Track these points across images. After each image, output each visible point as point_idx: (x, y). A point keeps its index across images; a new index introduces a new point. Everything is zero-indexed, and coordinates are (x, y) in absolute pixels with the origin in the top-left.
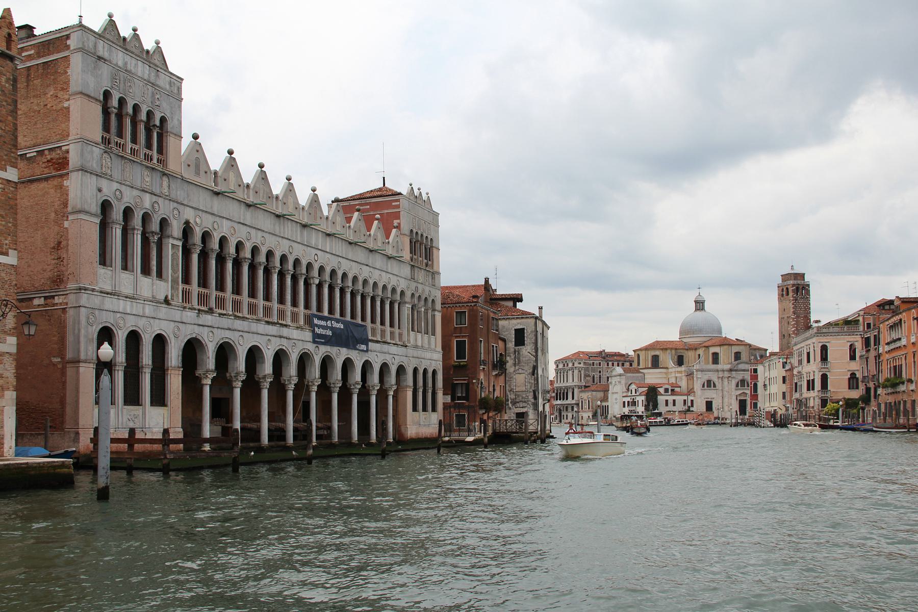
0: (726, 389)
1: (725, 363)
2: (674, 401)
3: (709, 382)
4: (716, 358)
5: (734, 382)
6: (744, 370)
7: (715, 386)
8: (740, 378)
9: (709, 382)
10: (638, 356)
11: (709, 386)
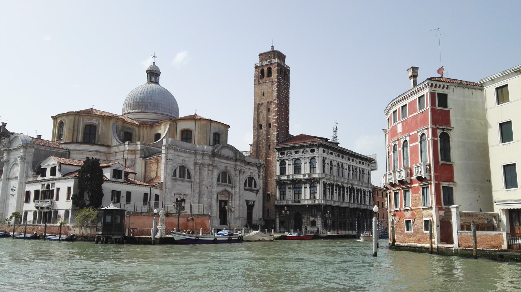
0: (206, 182)
1: (201, 144)
2: (129, 194)
3: (183, 168)
4: (187, 135)
5: (216, 173)
6: (228, 158)
7: (189, 177)
8: (222, 168)
9: (183, 168)
10: (61, 124)
11: (182, 176)
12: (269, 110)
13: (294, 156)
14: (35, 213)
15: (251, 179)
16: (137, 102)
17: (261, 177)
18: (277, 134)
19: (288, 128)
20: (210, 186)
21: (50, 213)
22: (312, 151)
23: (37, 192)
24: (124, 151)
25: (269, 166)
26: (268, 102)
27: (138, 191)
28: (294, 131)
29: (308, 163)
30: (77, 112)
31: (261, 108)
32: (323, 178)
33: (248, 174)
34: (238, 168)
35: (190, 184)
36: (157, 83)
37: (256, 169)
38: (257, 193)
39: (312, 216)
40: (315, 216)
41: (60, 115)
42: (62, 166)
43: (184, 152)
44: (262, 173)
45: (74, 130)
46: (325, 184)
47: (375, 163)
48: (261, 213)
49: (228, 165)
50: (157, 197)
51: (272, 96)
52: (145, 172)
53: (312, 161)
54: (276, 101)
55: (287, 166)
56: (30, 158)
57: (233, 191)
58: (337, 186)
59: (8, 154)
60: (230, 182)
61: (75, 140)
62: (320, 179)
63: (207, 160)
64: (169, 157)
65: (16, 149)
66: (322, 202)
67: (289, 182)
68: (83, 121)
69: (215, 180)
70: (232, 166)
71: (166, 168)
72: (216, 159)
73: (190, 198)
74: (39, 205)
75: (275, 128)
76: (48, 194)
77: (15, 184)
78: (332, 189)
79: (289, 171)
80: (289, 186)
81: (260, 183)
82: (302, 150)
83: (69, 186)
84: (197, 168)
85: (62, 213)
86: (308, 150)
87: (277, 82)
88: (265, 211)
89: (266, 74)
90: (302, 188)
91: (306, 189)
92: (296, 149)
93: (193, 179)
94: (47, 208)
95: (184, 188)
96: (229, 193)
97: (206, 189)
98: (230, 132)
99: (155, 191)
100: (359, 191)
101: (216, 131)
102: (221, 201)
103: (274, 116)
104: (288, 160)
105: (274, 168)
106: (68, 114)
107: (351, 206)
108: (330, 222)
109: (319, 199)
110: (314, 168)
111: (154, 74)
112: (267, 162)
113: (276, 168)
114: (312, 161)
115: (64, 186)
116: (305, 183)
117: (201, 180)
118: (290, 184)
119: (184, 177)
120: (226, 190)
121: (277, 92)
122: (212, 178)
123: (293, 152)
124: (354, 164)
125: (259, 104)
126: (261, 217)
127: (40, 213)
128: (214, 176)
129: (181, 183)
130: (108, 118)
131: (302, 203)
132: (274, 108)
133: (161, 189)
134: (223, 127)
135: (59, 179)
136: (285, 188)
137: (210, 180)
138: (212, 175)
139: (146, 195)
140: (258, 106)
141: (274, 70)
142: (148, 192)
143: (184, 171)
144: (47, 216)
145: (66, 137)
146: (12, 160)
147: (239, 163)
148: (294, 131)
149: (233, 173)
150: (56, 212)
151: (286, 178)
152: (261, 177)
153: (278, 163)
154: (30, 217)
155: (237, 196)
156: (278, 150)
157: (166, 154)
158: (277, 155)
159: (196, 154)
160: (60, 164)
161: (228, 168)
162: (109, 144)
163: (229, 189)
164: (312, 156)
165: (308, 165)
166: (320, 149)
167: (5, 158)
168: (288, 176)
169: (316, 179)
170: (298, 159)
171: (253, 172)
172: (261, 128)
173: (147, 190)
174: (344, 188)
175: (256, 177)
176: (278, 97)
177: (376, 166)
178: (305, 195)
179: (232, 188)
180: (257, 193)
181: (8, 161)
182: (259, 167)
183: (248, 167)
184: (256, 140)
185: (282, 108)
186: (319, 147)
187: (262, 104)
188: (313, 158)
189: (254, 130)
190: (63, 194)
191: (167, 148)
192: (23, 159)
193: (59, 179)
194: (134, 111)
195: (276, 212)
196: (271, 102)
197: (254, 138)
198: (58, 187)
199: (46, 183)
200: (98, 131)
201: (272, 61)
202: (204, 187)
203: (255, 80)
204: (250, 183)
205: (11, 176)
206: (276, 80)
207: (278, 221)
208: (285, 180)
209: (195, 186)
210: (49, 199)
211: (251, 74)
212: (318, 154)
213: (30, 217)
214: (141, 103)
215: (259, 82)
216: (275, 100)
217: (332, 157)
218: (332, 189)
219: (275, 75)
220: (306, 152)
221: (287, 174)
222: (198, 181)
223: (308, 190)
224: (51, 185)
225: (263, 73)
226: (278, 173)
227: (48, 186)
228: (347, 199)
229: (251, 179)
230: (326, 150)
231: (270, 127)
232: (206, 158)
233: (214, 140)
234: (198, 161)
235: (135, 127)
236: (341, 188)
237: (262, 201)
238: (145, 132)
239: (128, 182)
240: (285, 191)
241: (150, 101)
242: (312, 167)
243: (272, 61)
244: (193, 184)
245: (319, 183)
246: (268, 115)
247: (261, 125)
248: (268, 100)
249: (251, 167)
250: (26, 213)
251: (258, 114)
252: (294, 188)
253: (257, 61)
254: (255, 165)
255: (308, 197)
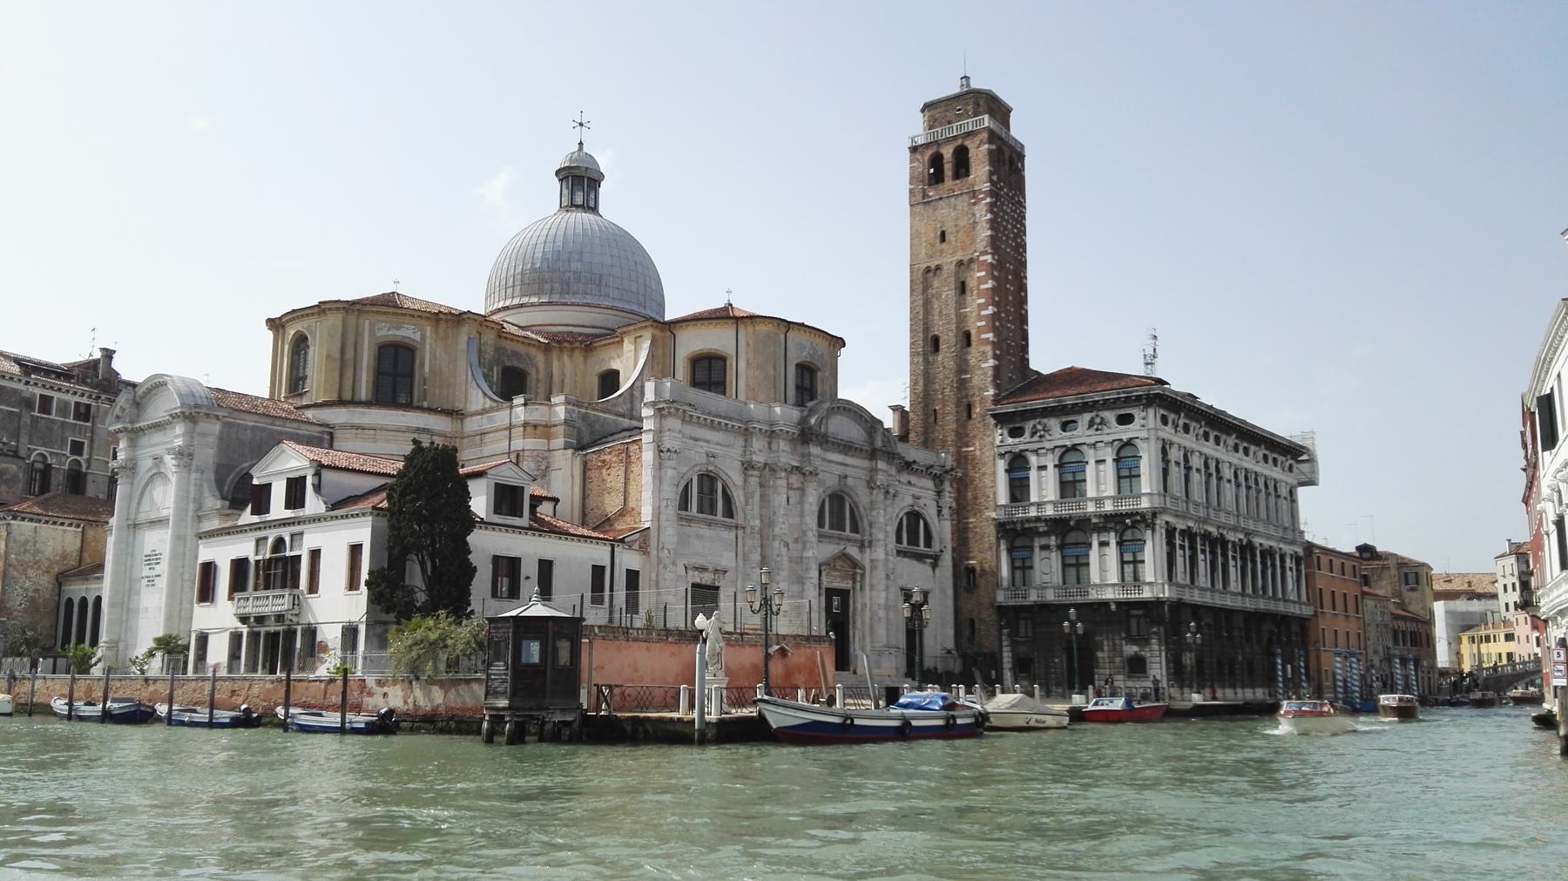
0: (781, 528)
2: (546, 567)
3: (708, 480)
6: (846, 447)
7: (729, 512)
8: (832, 482)
9: (708, 480)
10: (301, 342)
11: (707, 506)
12: (962, 288)
13: (1058, 436)
14: (236, 638)
15: (914, 516)
16: (533, 270)
17: (946, 512)
18: (996, 368)
19: (1025, 348)
20: (796, 540)
21: (290, 634)
22: (1125, 420)
23: (239, 566)
24: (510, 427)
25: (971, 473)
26: (960, 263)
27: (575, 558)
28: (1044, 358)
29: (1109, 461)
30: (354, 303)
31: (936, 283)
32: (1164, 510)
33: (905, 502)
34: (881, 479)
35: (733, 534)
36: (594, 209)
37: (929, 483)
38: (934, 566)
39: (1132, 640)
40: (1143, 641)
41: (296, 315)
42: (326, 474)
43: (713, 426)
44: (948, 499)
45: (344, 362)
46: (1170, 532)
47: (1312, 460)
48: (951, 632)
49: (849, 471)
50: (633, 577)
51: (973, 241)
52: (584, 497)
53: (1125, 456)
54: (989, 258)
55: (1033, 474)
56: (207, 454)
57: (865, 558)
58: (1206, 536)
59: (133, 445)
60: (855, 529)
61: (347, 396)
62: (1154, 515)
63: (785, 454)
64: (668, 443)
65: (158, 426)
66: (1166, 593)
67: (1042, 527)
68: (372, 332)
69: (812, 520)
70: (861, 473)
71: (658, 479)
72: (815, 450)
73: (734, 583)
74: (251, 608)
75: (989, 348)
76: (280, 571)
77: (158, 541)
78: (1193, 548)
79: (1040, 488)
80: (1044, 541)
81: (943, 530)
82: (1087, 417)
83: (355, 541)
84: (754, 481)
85: (331, 635)
86: (1110, 416)
87: (992, 193)
88: (965, 626)
89: (948, 168)
90: (1090, 545)
91: (1107, 550)
92: (1066, 414)
93: (739, 518)
94: (280, 618)
95: (713, 546)
96: (854, 564)
97: (784, 551)
98: (845, 359)
99: (629, 559)
100: (1268, 553)
101: (804, 356)
102: (830, 593)
103: (982, 307)
104: (1036, 451)
105: (987, 481)
106: (323, 308)
107: (1249, 604)
108: (1188, 659)
109: (1153, 582)
110: (1131, 476)
111: (580, 181)
112: (962, 459)
113: (994, 481)
114: (1125, 456)
115: (338, 543)
116: (1100, 529)
117: (768, 523)
118: (1046, 534)
119: (713, 512)
120: (844, 556)
121: (992, 228)
122: (802, 515)
123: (1054, 424)
124: (1248, 463)
125: (928, 270)
126: (951, 644)
127: (254, 636)
128: (807, 506)
129: (705, 531)
130: (449, 320)
131: (1094, 596)
132: (981, 281)
133: (644, 549)
134: (822, 346)
135: (316, 519)
136: (1031, 548)
137: (797, 520)
138: (801, 503)
139: (598, 571)
140: (925, 279)
141: (979, 154)
142: (607, 562)
143: (713, 491)
144: (279, 645)
145: (318, 383)
146: (146, 464)
147: (881, 465)
148: (1044, 358)
149: (863, 496)
150: (311, 632)
151: (1033, 513)
152: (946, 512)
153: (1001, 465)
154: (218, 652)
155: (880, 573)
156: (1001, 419)
157: (658, 433)
158: (999, 436)
159: (747, 433)
160: (320, 468)
161: (850, 481)
162: (459, 406)
163: (853, 551)
164: (1125, 437)
165: (1109, 469)
166: (1151, 411)
167: (121, 456)
168: (1039, 505)
169: (1143, 515)
170: (1075, 448)
171: (919, 493)
172: (937, 349)
173: (600, 554)
174: (1223, 542)
175: (930, 512)
176: (994, 241)
177: (1314, 471)
178: (1103, 570)
179: (862, 547)
180: (934, 566)
181: (131, 467)
182: (938, 479)
183: (905, 477)
184: (920, 388)
185: (1007, 281)
186: (1147, 406)
187: (938, 268)
188: (1129, 443)
189: (913, 355)
190: (334, 569)
191: (660, 413)
192: (185, 456)
193: (316, 519)
194: (525, 300)
195: (1001, 628)
196: (971, 261)
197: (914, 384)
198: (314, 546)
199: (272, 535)
200: (422, 365)
201: (969, 124)
202: (776, 544)
203: (911, 192)
204: (913, 527)
205: (142, 517)
206: (986, 186)
207: (1007, 657)
208: (1029, 520)
209: (749, 542)
210: (284, 586)
211: (898, 173)
212: (1145, 427)
213: (218, 652)
214: (545, 274)
215: (925, 195)
216: (984, 253)
217: (1188, 441)
218: (1193, 548)
219: (980, 171)
220: (1103, 422)
221: (1034, 498)
222: (757, 523)
223: (1112, 551)
224: (287, 539)
225: (938, 168)
226: (1003, 497)
227: (279, 544)
228: (1235, 585)
229: (914, 516)
230: (1171, 417)
231: (969, 344)
232: (783, 445)
233: (799, 388)
234: (755, 458)
235: (533, 351)
236: (1217, 544)
237: (950, 592)
238: (565, 366)
239: (541, 527)
240: (1031, 558)
241: (576, 266)
242: (1125, 473)
243: (969, 124)
244: (740, 532)
245: (1152, 526)
246: (960, 304)
247: (936, 341)
248: (959, 256)
249: (913, 479)
250: (203, 639)
251: (927, 304)
252: (1061, 547)
253: (917, 128)
254: (927, 471)
255: (1113, 577)
